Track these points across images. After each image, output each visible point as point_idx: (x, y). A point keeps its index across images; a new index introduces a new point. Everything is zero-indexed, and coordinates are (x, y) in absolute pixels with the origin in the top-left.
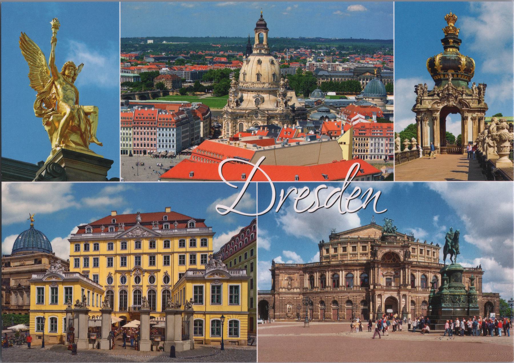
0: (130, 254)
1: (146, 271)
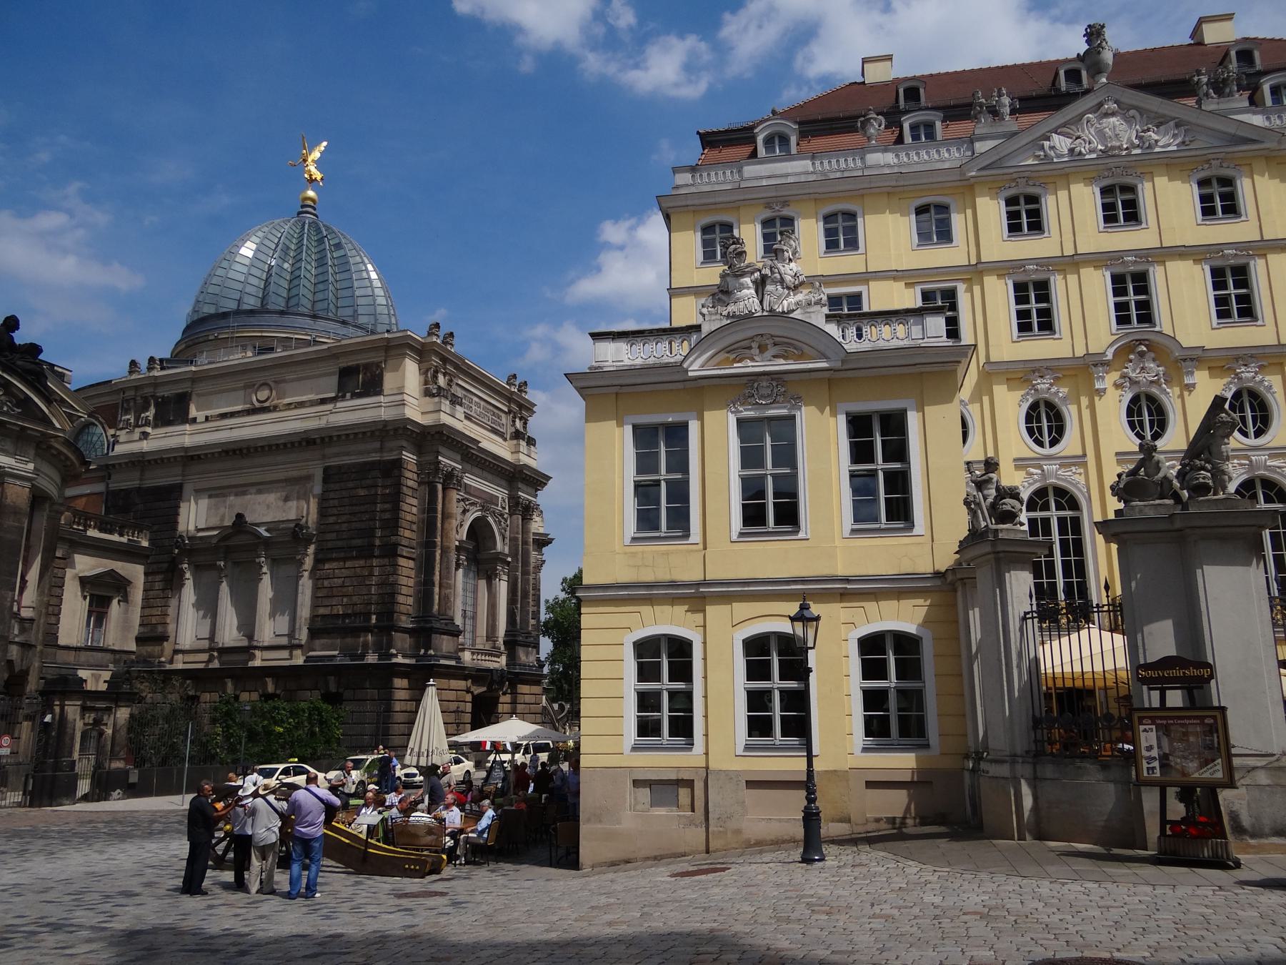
0: (1073, 263)
1: (1198, 358)
